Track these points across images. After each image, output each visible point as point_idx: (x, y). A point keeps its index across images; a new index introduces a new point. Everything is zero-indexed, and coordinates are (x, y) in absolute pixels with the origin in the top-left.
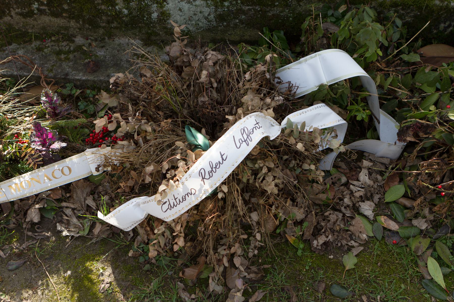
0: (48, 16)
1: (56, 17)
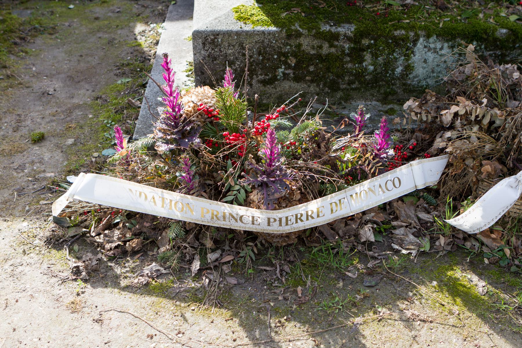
0: (290, 81)
1: (298, 82)
